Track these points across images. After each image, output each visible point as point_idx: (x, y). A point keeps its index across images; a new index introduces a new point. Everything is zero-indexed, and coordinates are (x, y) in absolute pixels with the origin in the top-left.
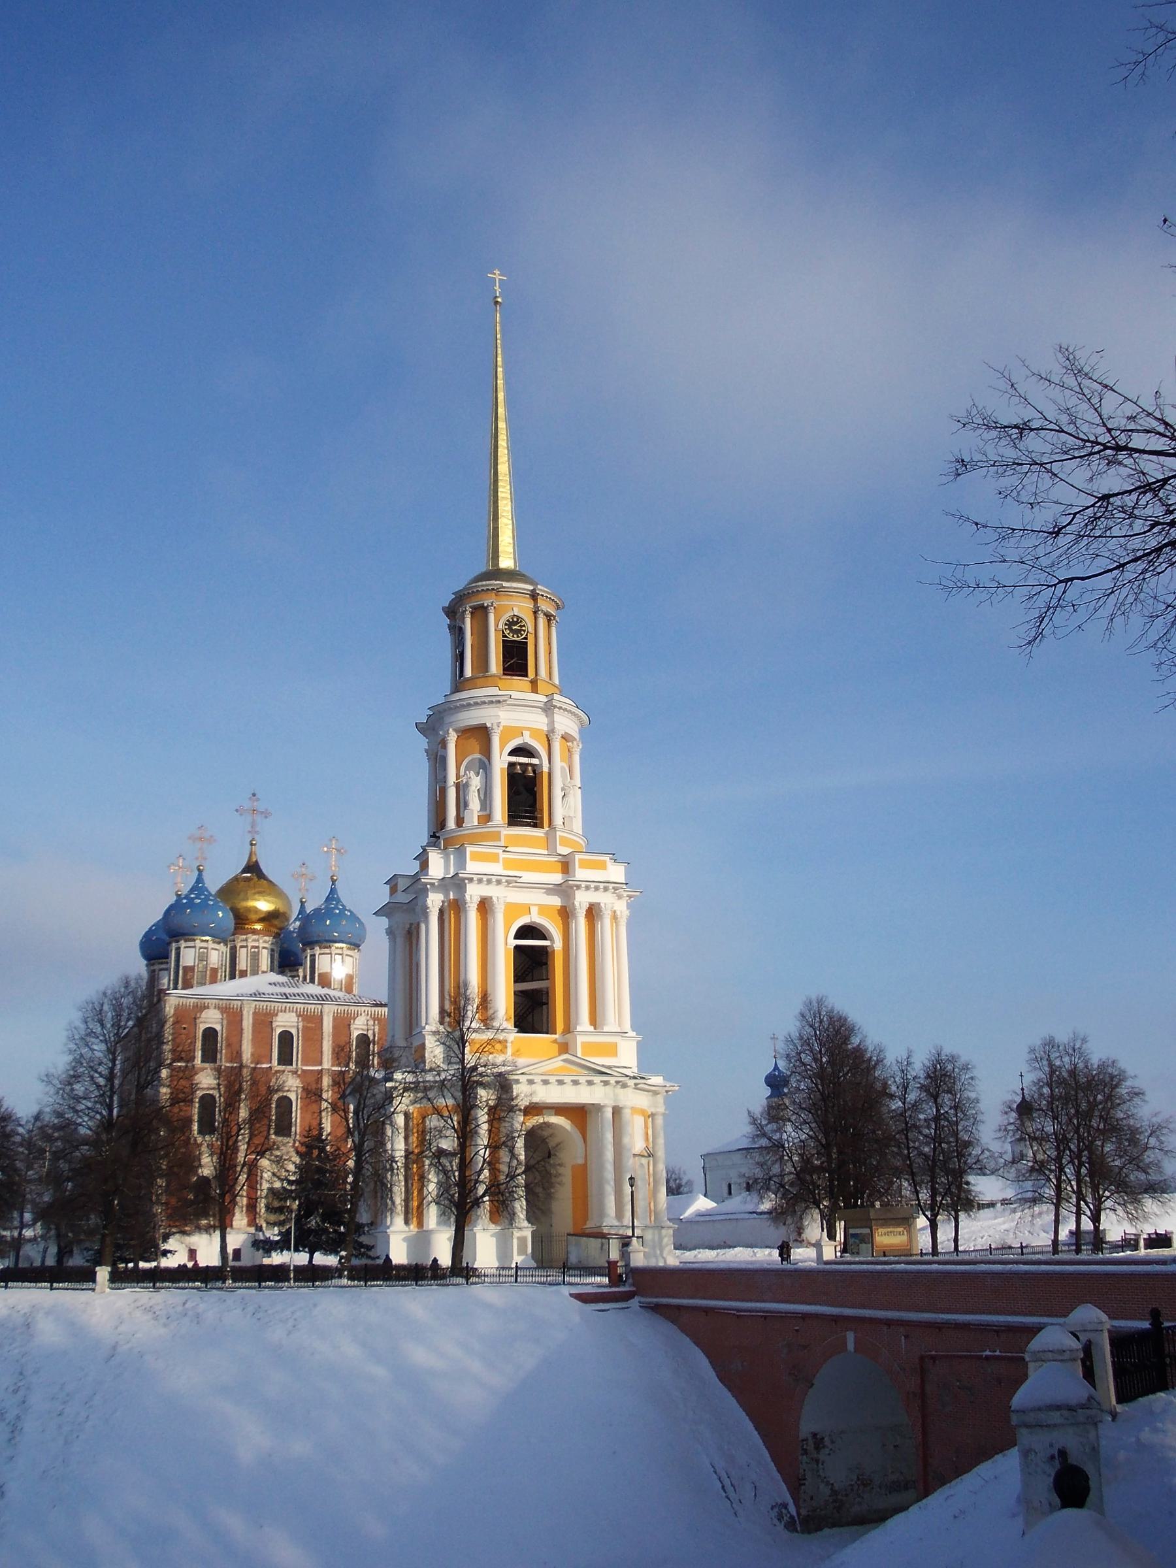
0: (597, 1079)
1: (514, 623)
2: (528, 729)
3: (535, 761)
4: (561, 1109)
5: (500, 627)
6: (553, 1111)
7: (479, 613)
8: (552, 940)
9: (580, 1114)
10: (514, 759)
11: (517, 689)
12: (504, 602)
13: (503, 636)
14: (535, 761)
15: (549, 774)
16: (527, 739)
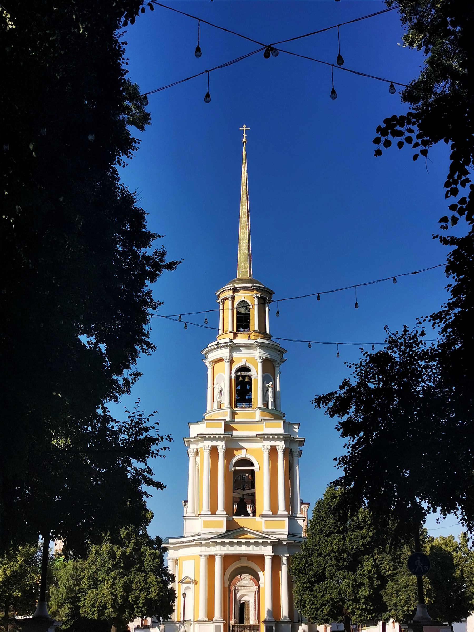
0: (260, 541)
1: (244, 304)
2: (244, 358)
3: (250, 373)
4: (250, 557)
5: (235, 306)
7: (226, 302)
8: (252, 465)
9: (260, 559)
10: (239, 374)
11: (241, 339)
12: (236, 295)
13: (237, 312)
14: (250, 373)
15: (257, 380)
16: (243, 363)
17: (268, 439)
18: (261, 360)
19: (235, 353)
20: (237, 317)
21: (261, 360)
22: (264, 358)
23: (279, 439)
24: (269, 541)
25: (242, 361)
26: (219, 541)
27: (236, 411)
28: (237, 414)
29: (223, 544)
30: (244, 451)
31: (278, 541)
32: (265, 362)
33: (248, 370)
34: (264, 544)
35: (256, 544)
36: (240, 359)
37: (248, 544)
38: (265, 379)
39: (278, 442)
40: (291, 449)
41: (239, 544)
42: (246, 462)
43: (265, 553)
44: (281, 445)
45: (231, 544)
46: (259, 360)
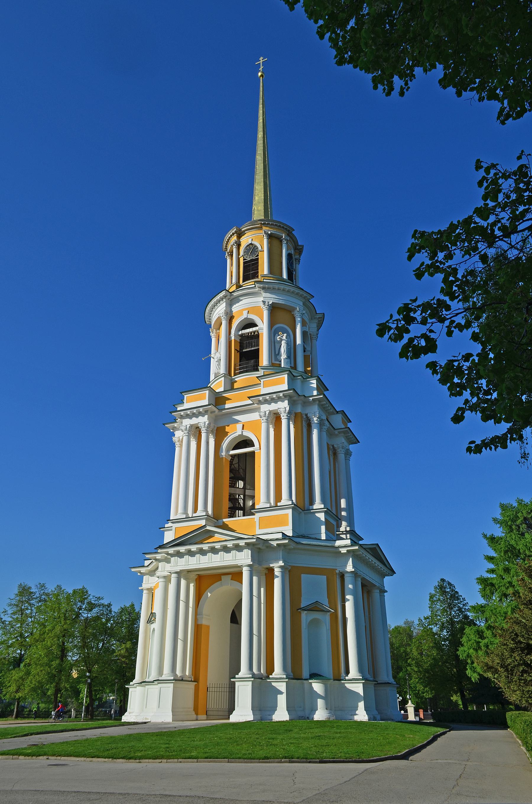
6: (230, 576)
16: (245, 315)
17: (266, 402)
18: (266, 306)
19: (235, 306)
20: (244, 267)
21: (266, 306)
22: (270, 303)
23: (279, 399)
24: (242, 543)
25: (242, 314)
26: (171, 551)
27: (236, 379)
28: (236, 382)
29: (179, 555)
30: (239, 426)
31: (255, 540)
32: (273, 309)
33: (253, 324)
34: (238, 548)
35: (226, 549)
36: (241, 312)
37: (214, 551)
38: (273, 331)
39: (280, 403)
40: (306, 415)
41: (202, 552)
42: (247, 443)
43: (239, 563)
44: (283, 406)
45: (191, 554)
46: (264, 307)
